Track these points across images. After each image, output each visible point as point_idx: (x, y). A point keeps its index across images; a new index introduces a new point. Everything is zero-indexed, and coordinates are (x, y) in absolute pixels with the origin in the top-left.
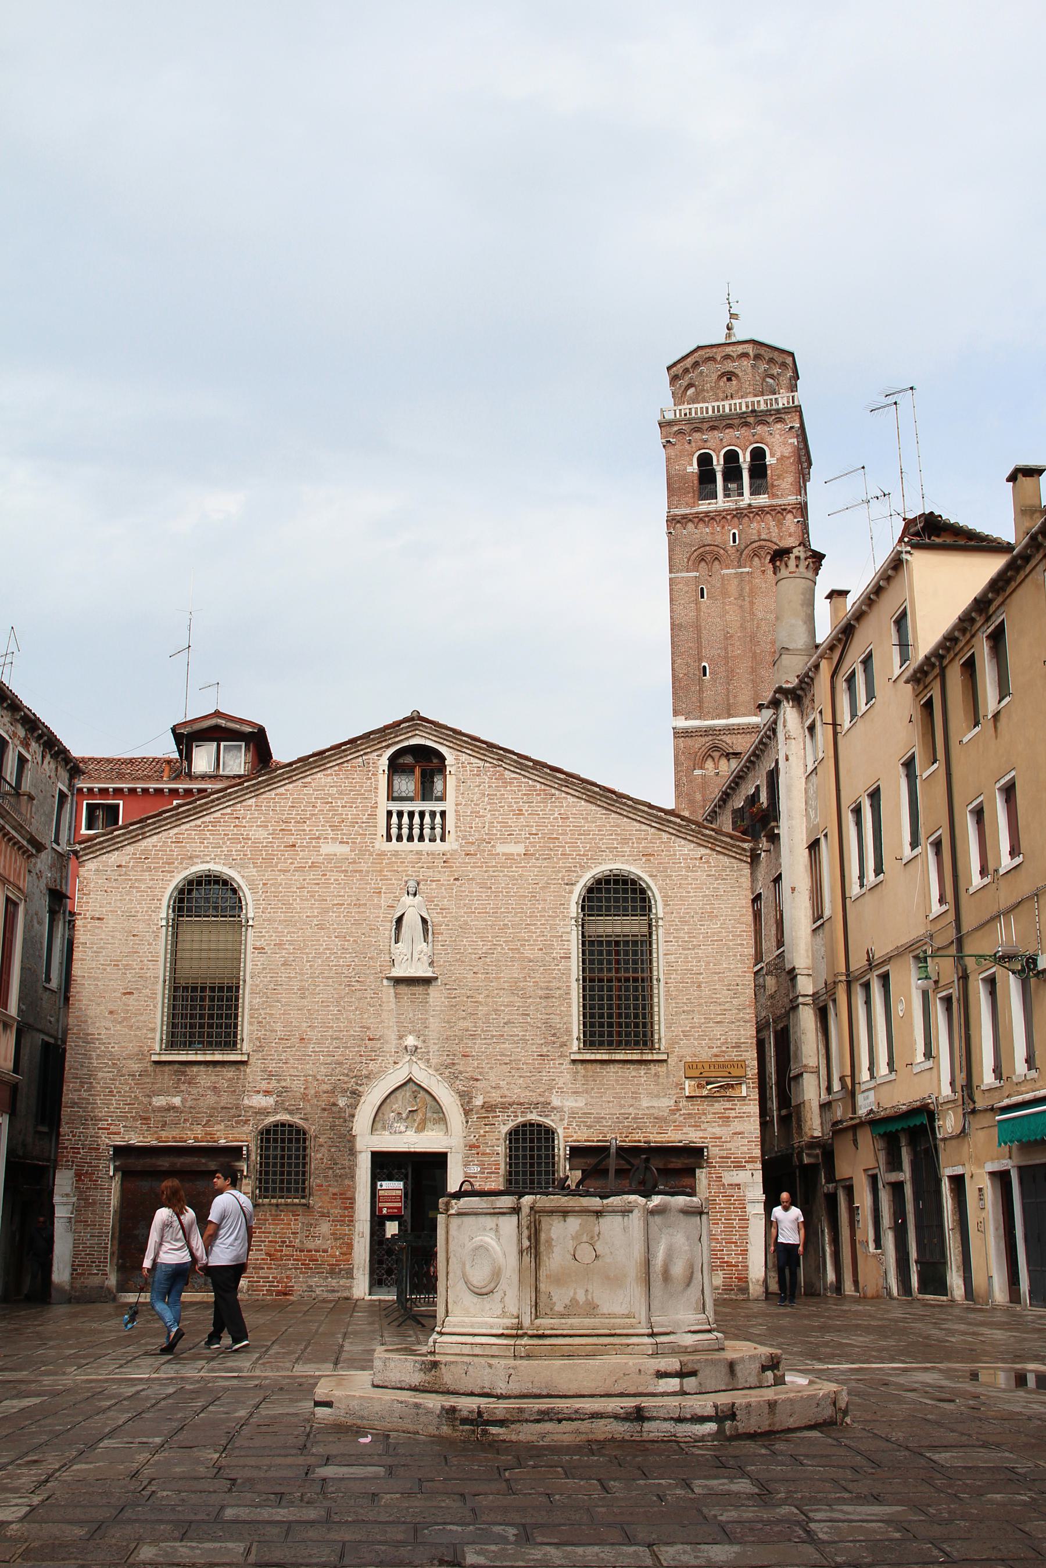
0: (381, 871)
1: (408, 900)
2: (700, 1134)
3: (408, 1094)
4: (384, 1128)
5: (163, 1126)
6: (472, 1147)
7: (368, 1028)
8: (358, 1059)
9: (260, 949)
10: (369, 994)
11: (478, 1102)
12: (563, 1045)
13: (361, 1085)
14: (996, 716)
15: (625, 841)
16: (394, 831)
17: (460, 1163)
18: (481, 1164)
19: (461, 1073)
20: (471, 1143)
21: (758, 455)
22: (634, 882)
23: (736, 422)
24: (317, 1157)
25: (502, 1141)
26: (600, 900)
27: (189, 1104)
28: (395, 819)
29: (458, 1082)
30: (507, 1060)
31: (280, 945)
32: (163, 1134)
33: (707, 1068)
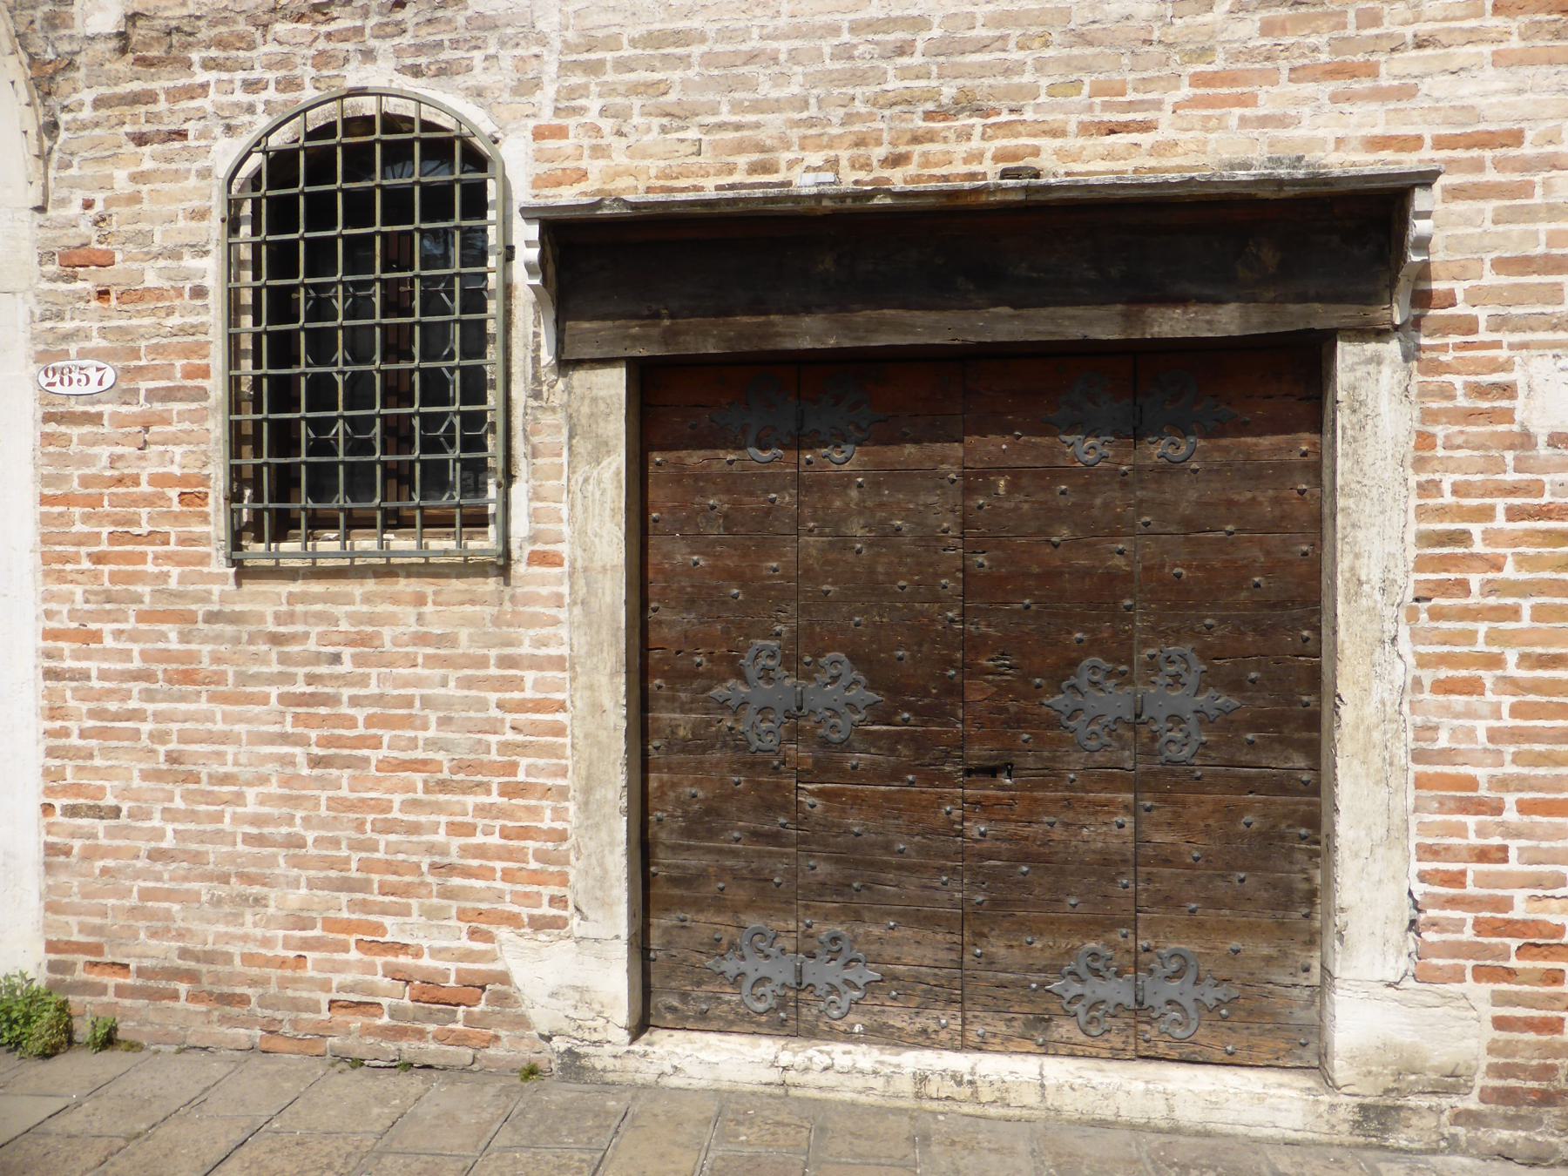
2: (1374, 119)
6: (74, 261)
17: (22, 348)
18: (123, 349)
25: (214, 227)
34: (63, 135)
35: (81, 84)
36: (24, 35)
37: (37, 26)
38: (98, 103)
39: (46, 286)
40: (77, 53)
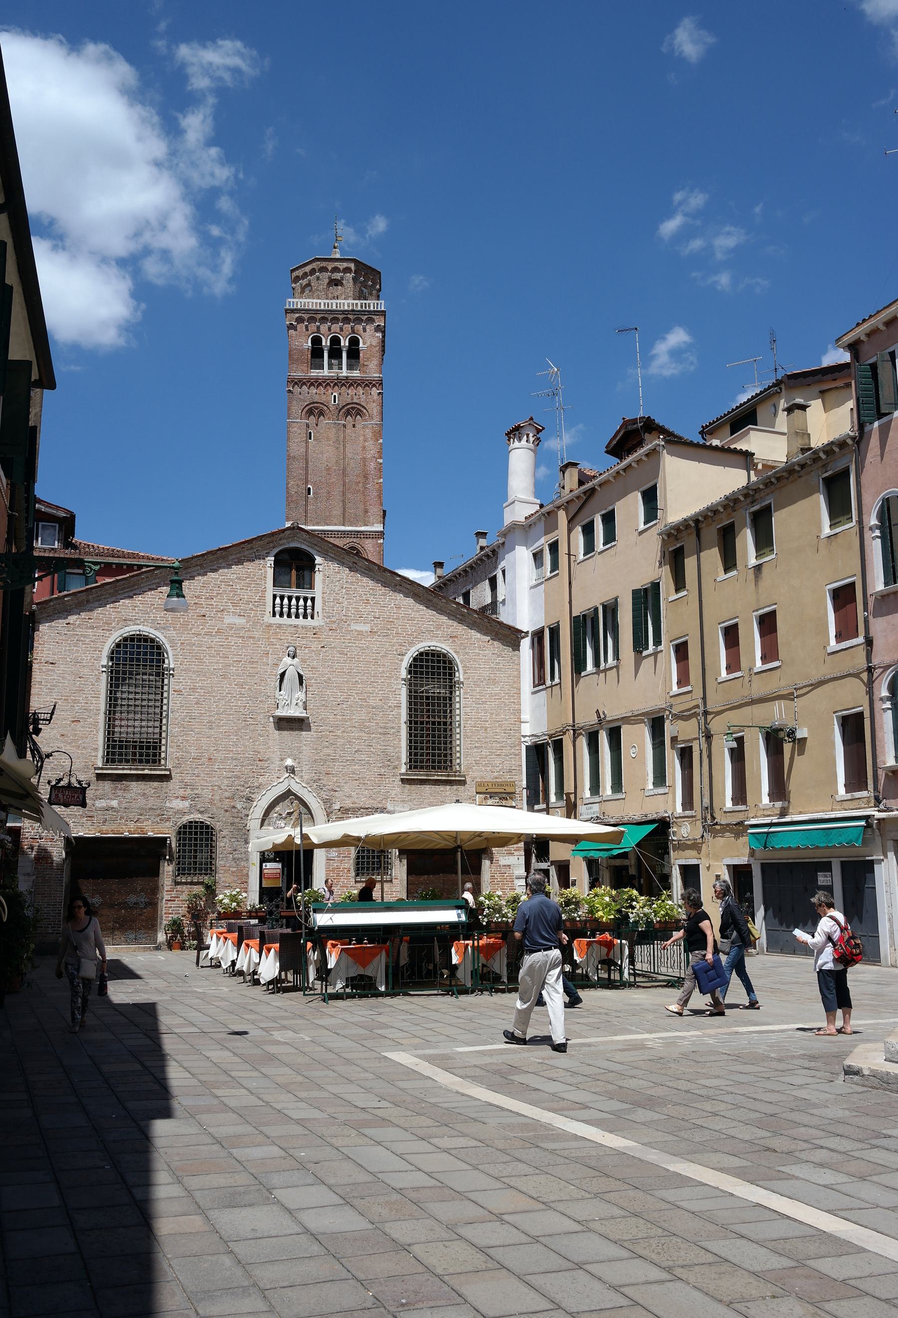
0: (268, 638)
1: (288, 660)
5: (105, 822)
7: (259, 752)
8: (251, 774)
9: (179, 692)
10: (260, 728)
11: (337, 806)
12: (395, 767)
14: (758, 568)
15: (438, 627)
16: (278, 609)
21: (354, 342)
22: (445, 655)
23: (341, 317)
24: (222, 845)
26: (421, 667)
27: (123, 806)
28: (278, 600)
30: (357, 777)
31: (194, 689)
32: (104, 828)
33: (490, 785)
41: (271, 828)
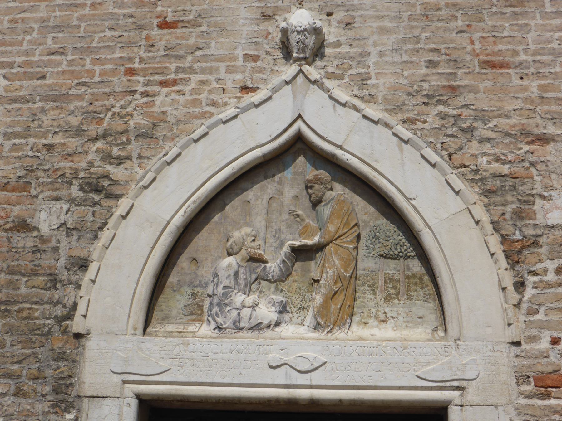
3: (289, 192)
4: (195, 313)
8: (119, 82)
13: (120, 161)
19: (482, 116)
20: (543, 366)
29: (474, 147)
34: (529, 292)
35: (544, 257)
36: (497, 222)
37: (507, 216)
38: (559, 271)
39: (523, 401)
40: (540, 236)
41: (206, 329)
